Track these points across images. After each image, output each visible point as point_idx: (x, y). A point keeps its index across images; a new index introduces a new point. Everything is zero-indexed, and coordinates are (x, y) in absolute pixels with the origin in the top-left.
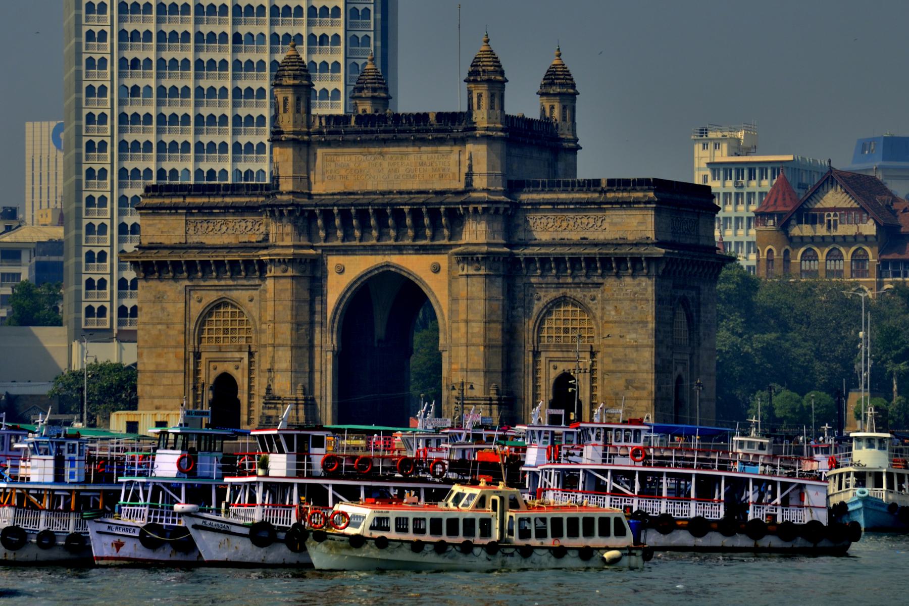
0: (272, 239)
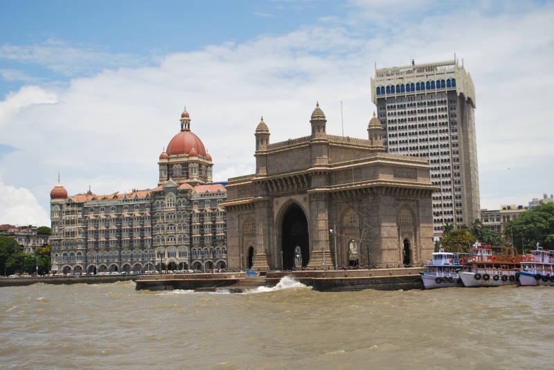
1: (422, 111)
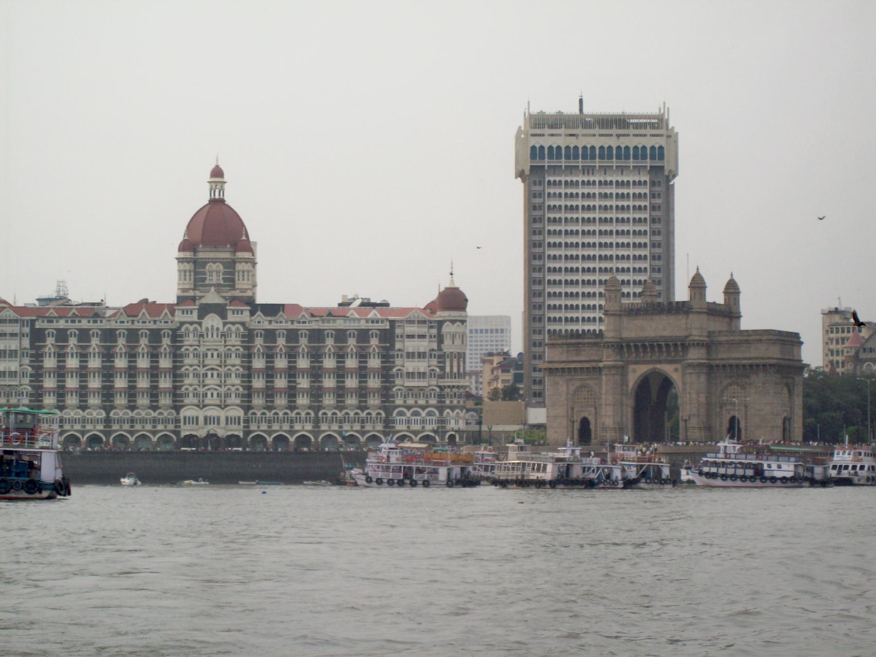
0: (604, 359)
1: (606, 196)
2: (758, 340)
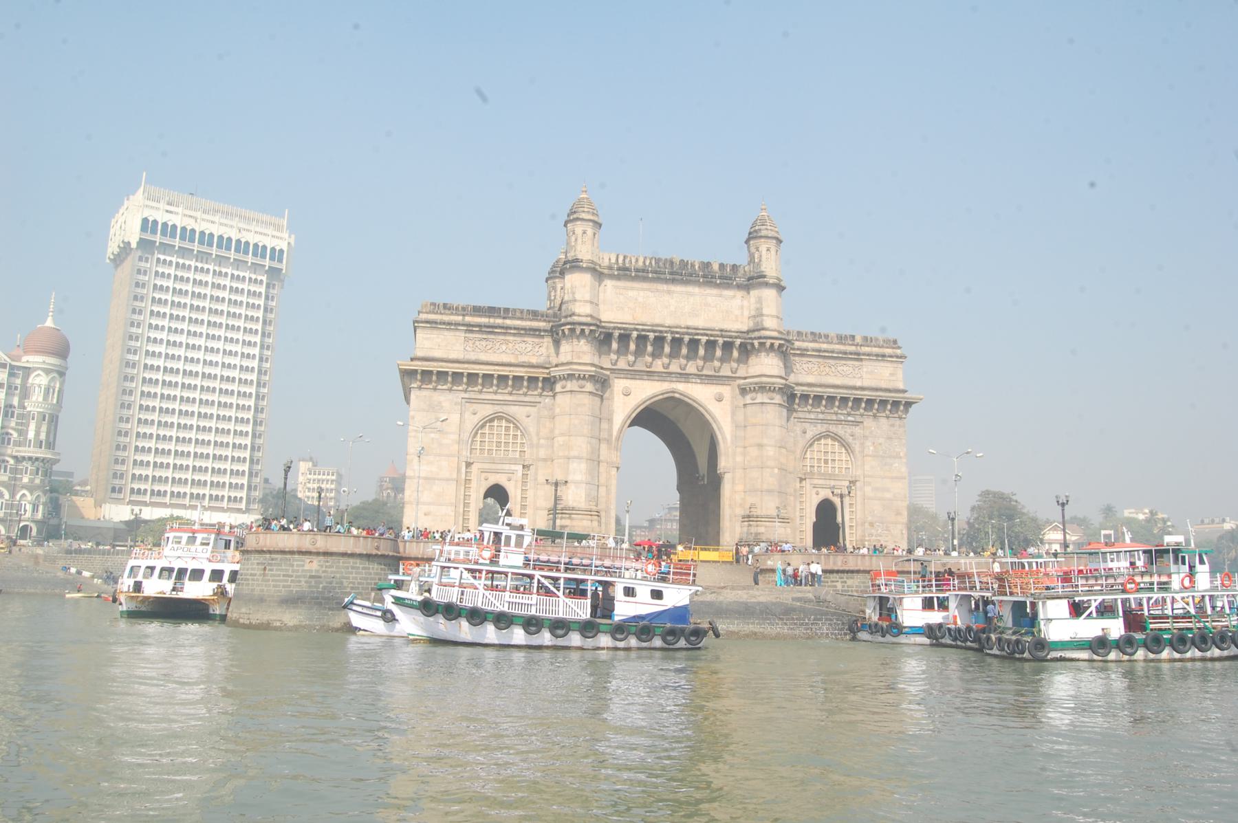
1: (219, 286)
2: (877, 355)
